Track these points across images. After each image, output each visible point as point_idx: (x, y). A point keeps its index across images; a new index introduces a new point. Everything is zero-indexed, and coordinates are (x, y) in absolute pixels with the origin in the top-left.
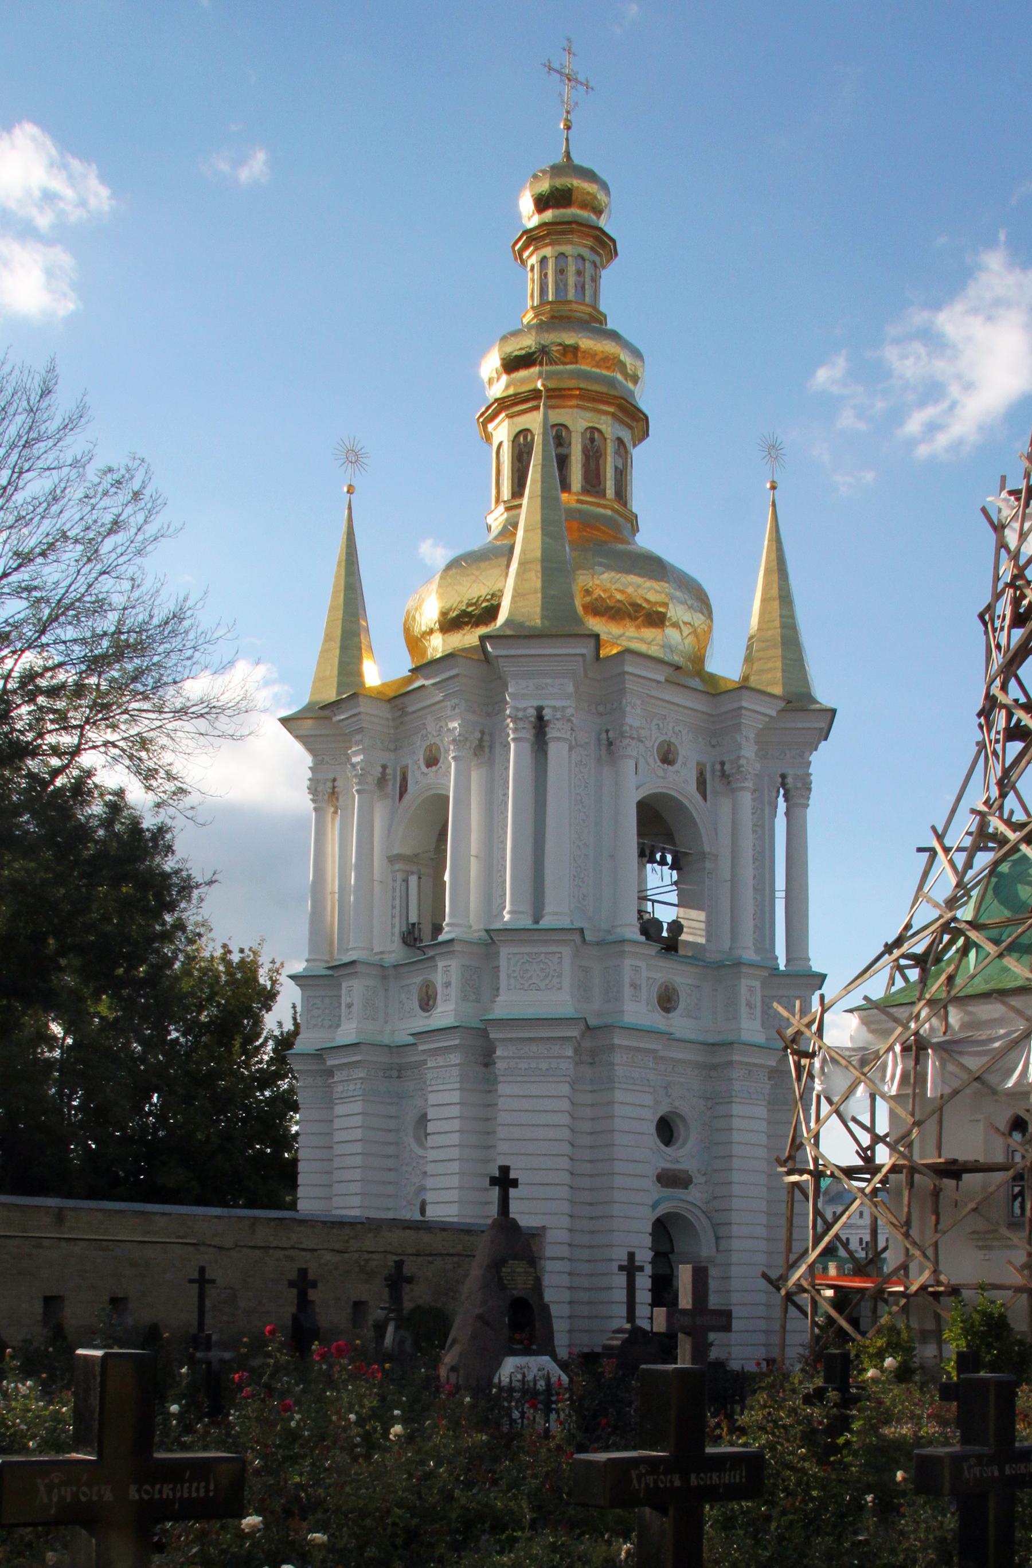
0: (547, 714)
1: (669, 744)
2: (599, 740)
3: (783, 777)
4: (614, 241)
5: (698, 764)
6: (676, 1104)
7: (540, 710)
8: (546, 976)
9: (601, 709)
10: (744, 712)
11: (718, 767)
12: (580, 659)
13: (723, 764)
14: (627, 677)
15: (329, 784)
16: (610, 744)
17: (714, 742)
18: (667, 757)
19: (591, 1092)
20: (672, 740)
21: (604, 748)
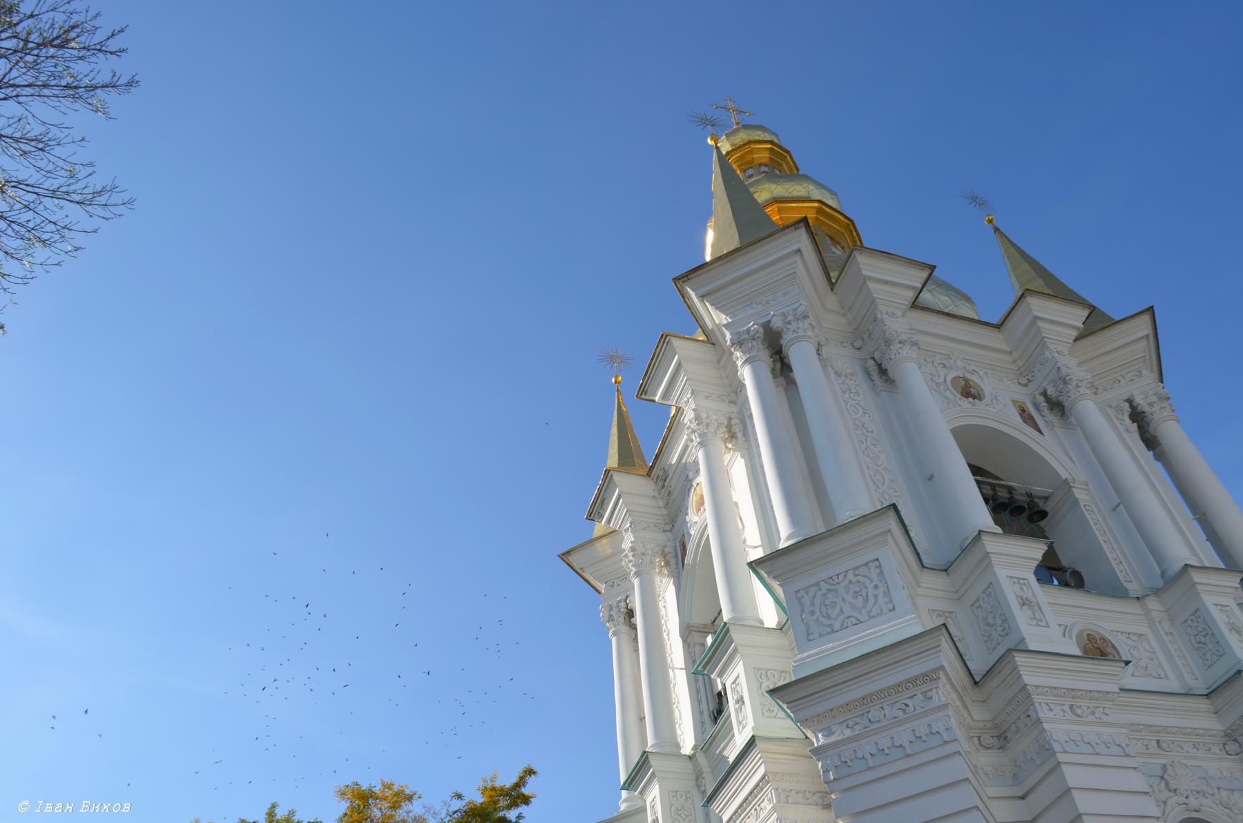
0: (777, 323)
1: (966, 380)
2: (867, 373)
3: (1130, 401)
4: (788, 152)
5: (1014, 402)
6: (1193, 802)
7: (767, 326)
8: (866, 599)
9: (858, 343)
10: (1040, 324)
11: (1041, 399)
12: (797, 258)
13: (1044, 394)
14: (871, 285)
15: (623, 604)
16: (883, 372)
17: (1024, 381)
18: (969, 391)
19: (1023, 798)
20: (968, 376)
21: (875, 376)
